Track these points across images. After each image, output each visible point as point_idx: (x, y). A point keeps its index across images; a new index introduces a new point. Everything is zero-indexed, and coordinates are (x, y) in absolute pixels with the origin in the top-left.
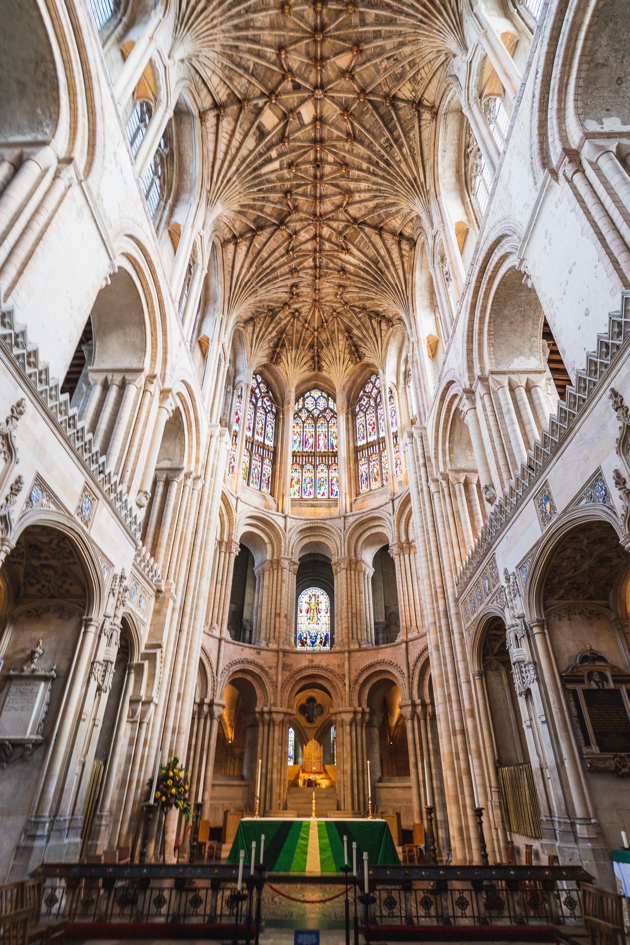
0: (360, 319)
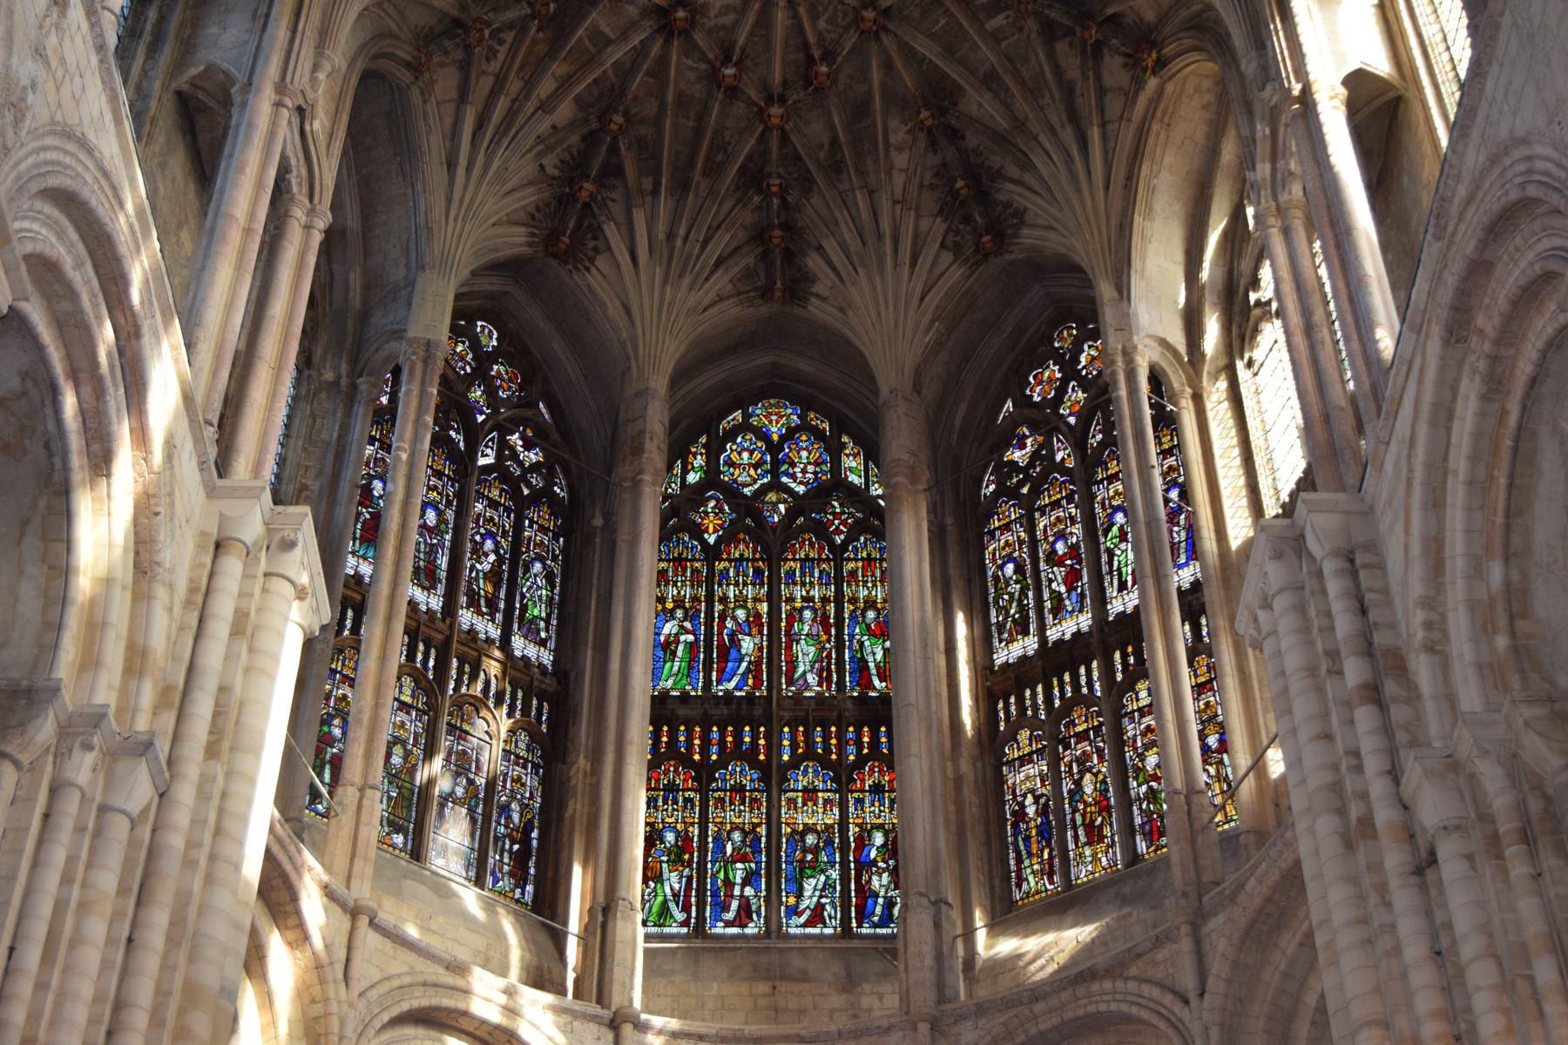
0: (995, 38)
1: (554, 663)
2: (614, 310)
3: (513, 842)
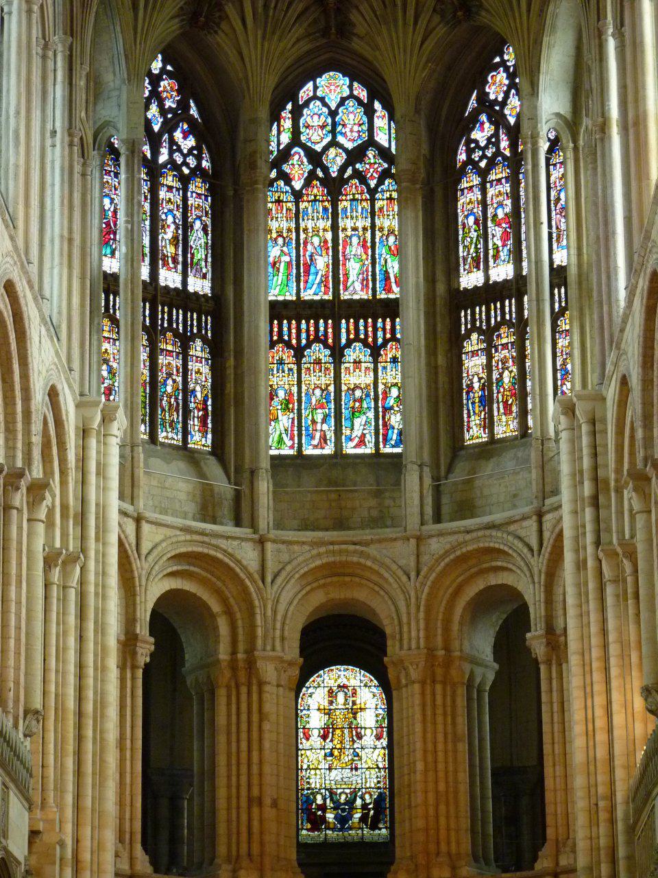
1: (212, 288)
2: (232, 55)
3: (199, 410)
